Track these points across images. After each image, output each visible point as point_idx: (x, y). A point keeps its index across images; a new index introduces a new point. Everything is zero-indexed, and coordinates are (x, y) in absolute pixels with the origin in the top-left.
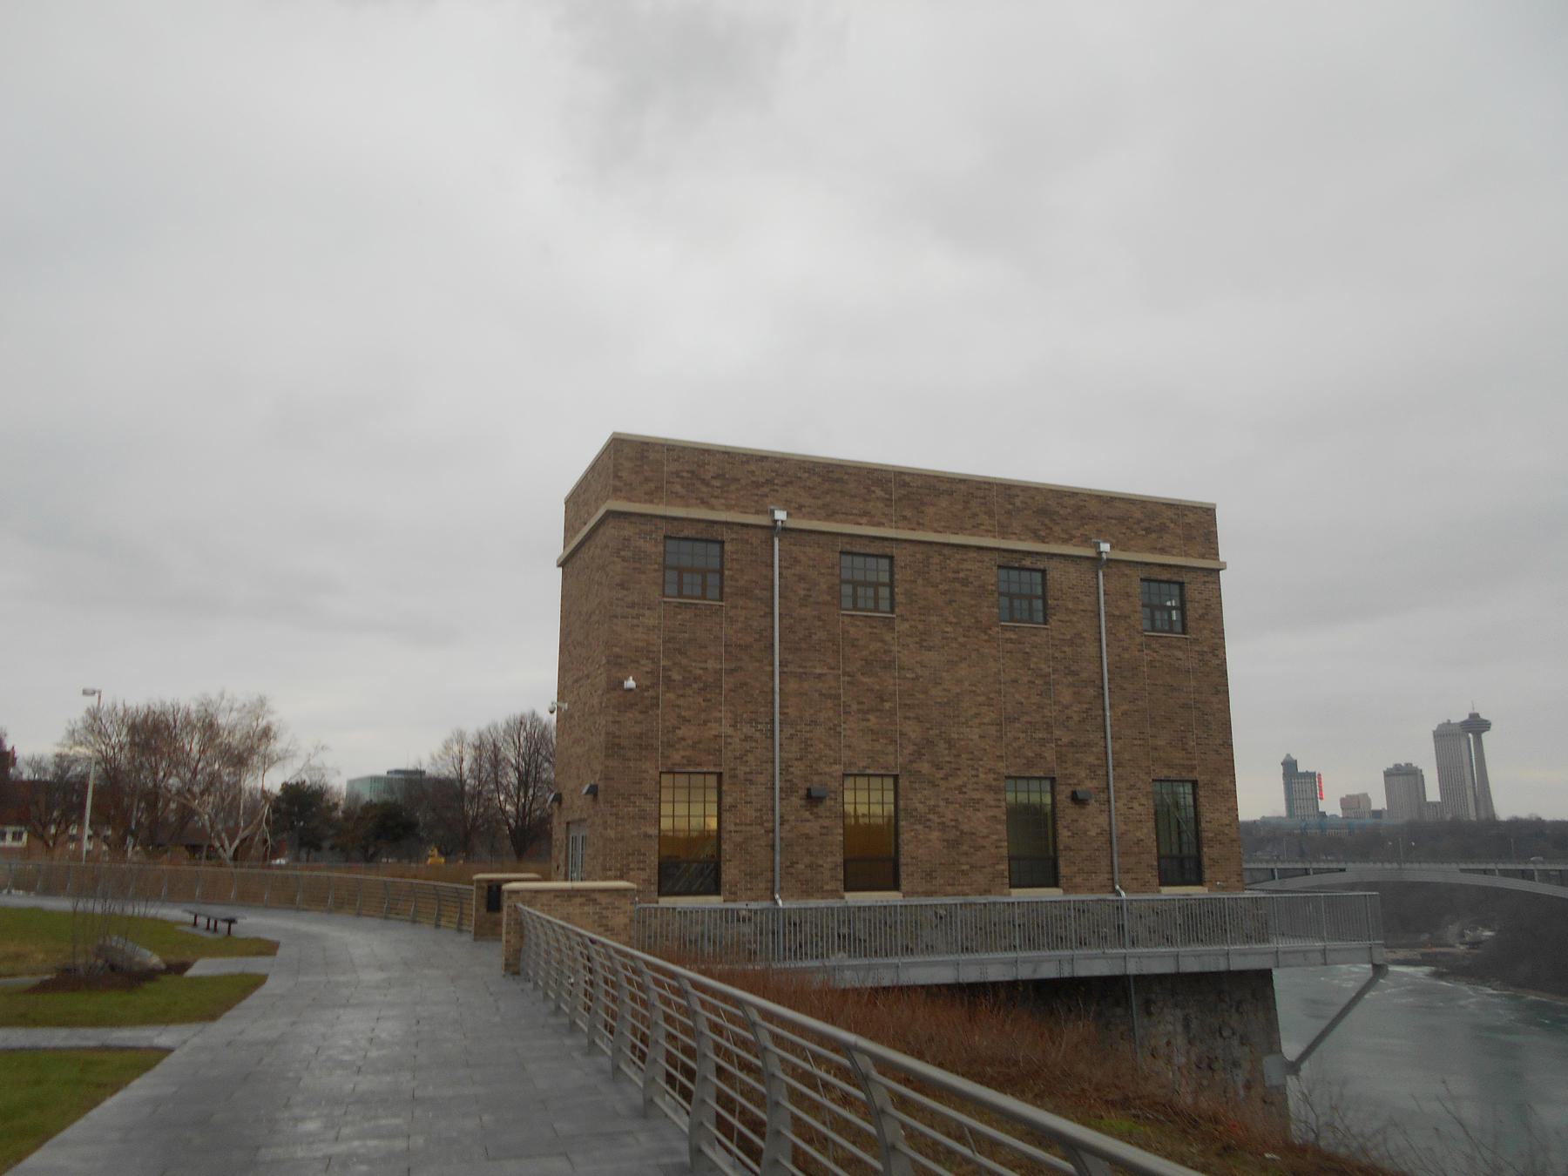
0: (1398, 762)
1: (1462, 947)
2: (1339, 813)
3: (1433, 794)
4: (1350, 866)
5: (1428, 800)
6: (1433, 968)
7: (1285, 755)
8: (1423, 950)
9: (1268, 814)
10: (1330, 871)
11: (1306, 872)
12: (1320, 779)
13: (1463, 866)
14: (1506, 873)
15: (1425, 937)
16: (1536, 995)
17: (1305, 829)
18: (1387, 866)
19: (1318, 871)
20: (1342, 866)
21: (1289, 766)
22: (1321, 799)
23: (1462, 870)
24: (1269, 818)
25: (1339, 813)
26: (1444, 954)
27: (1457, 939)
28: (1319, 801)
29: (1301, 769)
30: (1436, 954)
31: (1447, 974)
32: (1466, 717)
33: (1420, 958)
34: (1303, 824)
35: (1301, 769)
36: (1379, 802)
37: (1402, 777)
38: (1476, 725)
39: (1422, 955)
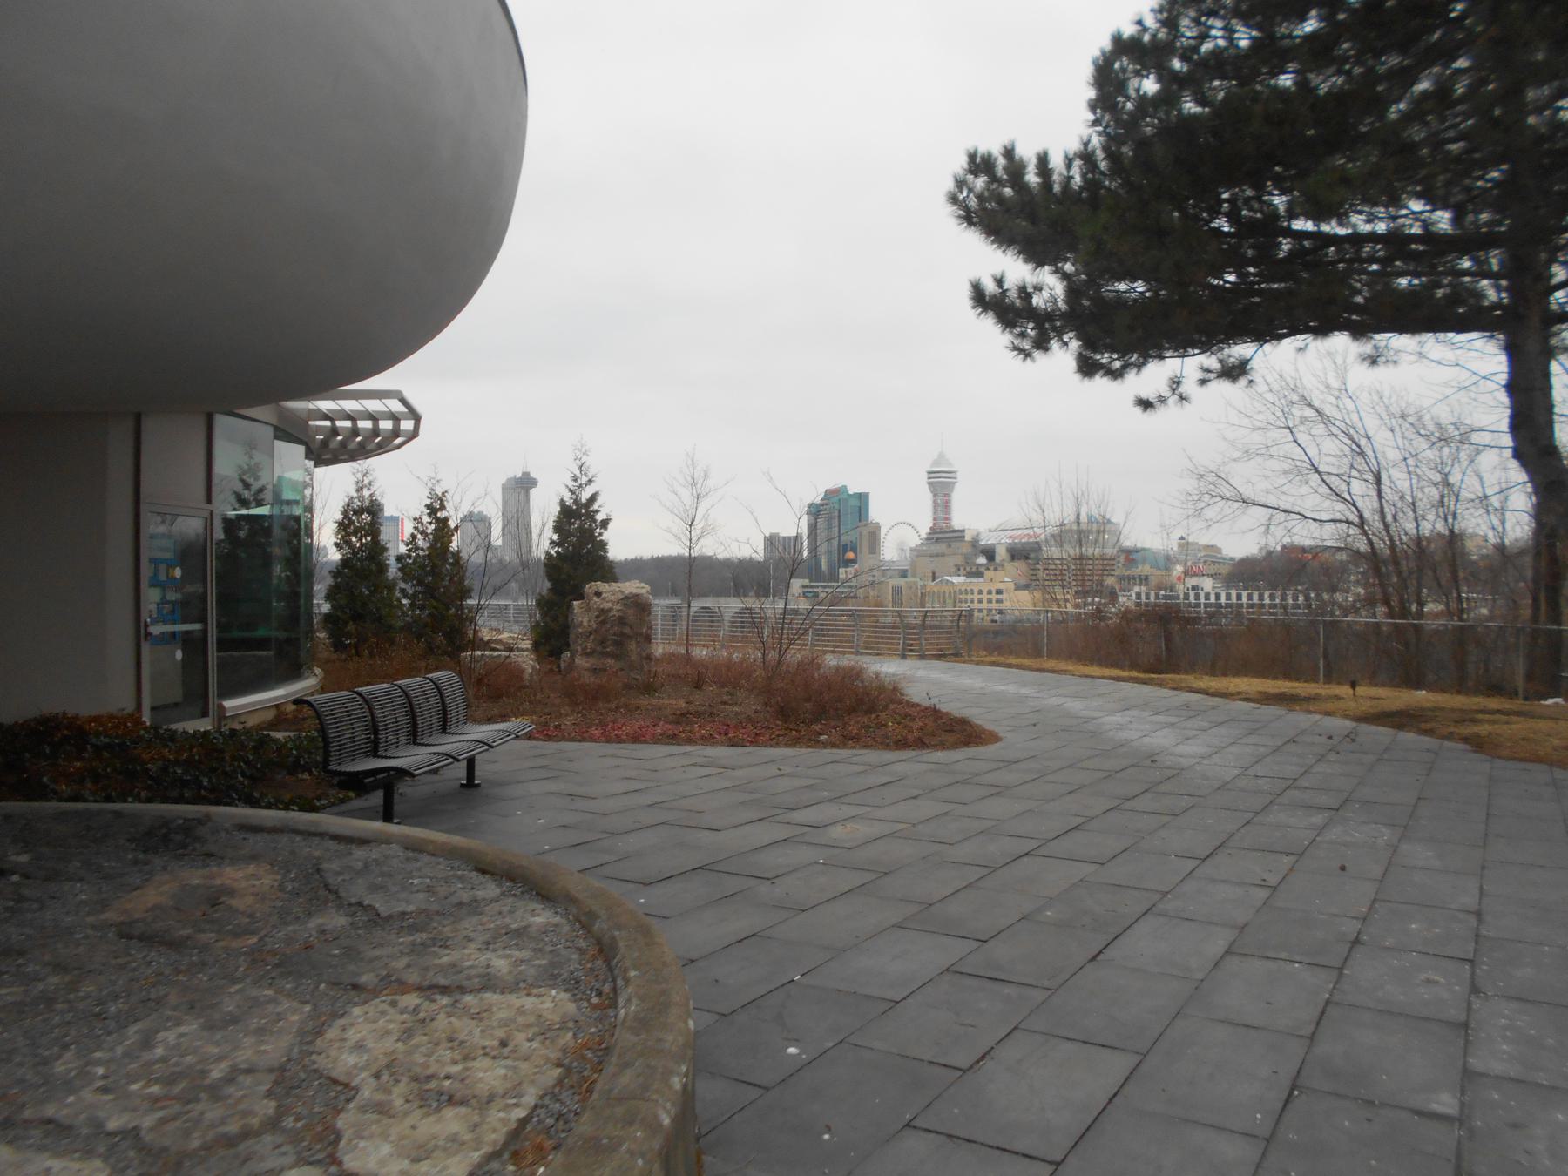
32: (519, 475)
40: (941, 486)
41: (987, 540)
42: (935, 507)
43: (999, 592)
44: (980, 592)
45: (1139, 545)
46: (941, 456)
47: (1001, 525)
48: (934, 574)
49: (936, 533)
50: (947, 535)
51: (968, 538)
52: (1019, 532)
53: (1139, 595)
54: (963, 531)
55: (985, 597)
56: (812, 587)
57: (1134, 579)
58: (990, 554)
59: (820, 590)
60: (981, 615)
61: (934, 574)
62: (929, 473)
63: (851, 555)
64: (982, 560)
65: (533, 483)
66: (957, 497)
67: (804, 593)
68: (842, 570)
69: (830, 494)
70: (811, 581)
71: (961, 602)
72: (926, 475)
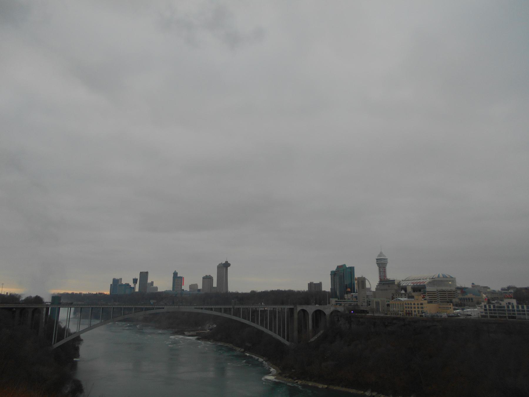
0: (207, 275)
1: (208, 330)
3: (215, 285)
4: (165, 307)
5: (213, 286)
6: (198, 337)
8: (197, 332)
9: (168, 289)
12: (183, 279)
13: (195, 307)
14: (206, 309)
15: (200, 328)
16: (220, 343)
17: (176, 294)
18: (176, 307)
20: (163, 307)
21: (175, 274)
22: (183, 285)
23: (195, 308)
24: (168, 291)
25: (188, 290)
26: (202, 333)
27: (208, 328)
28: (182, 286)
29: (178, 276)
30: (200, 333)
31: (201, 338)
32: (224, 262)
33: (196, 334)
35: (178, 276)
36: (200, 287)
37: (207, 279)
38: (227, 265)
39: (197, 333)
40: (382, 264)
41: (404, 284)
42: (380, 272)
43: (422, 304)
44: (414, 304)
45: (463, 286)
46: (381, 253)
47: (407, 278)
49: (383, 281)
50: (388, 282)
51: (396, 283)
52: (416, 281)
53: (485, 306)
54: (394, 280)
55: (416, 306)
56: (339, 301)
57: (469, 299)
58: (405, 289)
59: (342, 303)
60: (415, 313)
62: (377, 259)
63: (349, 290)
64: (403, 292)
66: (388, 268)
68: (346, 295)
69: (339, 267)
70: (338, 299)
71: (406, 308)
72: (376, 260)
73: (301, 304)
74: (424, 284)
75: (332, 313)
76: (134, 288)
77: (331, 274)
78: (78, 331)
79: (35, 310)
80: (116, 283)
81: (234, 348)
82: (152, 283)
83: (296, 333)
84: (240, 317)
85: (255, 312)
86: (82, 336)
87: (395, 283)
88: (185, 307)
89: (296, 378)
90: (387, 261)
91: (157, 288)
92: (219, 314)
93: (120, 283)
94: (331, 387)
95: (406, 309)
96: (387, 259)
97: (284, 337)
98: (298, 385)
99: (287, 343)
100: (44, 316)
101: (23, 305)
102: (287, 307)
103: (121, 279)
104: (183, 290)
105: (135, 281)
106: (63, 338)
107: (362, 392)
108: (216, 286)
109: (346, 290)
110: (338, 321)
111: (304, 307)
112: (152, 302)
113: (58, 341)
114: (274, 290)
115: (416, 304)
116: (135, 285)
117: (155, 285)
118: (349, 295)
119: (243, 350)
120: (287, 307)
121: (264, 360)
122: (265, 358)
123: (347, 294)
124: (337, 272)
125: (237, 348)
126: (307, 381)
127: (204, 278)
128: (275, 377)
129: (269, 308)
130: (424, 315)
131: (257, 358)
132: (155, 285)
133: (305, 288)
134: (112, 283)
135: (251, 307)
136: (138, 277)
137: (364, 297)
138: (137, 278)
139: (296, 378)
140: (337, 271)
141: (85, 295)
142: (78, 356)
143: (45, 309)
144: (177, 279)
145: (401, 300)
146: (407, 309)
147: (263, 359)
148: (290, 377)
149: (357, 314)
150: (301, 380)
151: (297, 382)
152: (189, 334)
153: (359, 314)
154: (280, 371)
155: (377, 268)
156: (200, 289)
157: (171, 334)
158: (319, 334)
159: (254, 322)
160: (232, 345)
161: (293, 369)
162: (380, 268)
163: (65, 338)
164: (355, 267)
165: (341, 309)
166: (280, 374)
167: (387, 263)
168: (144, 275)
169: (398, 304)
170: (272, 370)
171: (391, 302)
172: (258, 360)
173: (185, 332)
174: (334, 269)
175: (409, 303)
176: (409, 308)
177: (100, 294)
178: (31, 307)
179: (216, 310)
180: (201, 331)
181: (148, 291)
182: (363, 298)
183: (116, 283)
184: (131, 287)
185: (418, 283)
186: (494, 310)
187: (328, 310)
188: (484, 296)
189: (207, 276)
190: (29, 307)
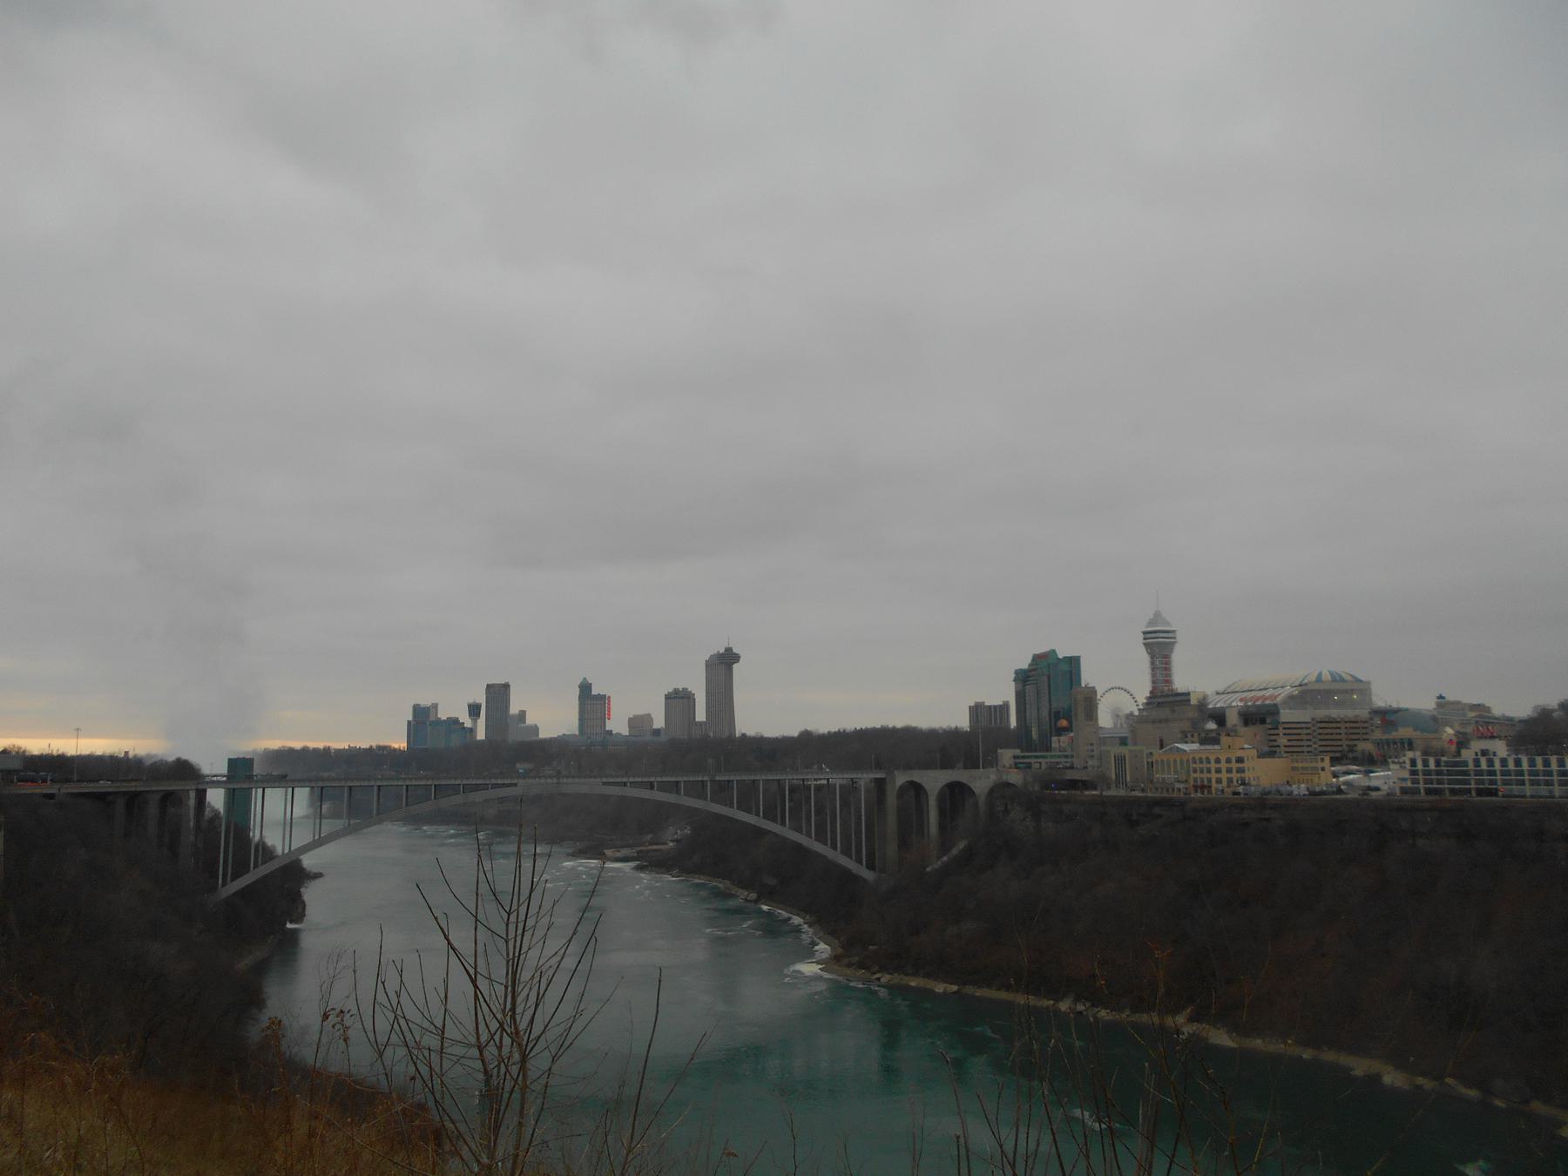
1: (671, 844)
2: (625, 731)
3: (701, 716)
4: (521, 782)
5: (697, 720)
6: (638, 862)
7: (582, 679)
10: (504, 785)
11: (485, 787)
12: (609, 701)
13: (604, 780)
16: (700, 879)
19: (495, 786)
20: (515, 781)
21: (585, 688)
25: (625, 731)
27: (672, 837)
30: (648, 851)
32: (722, 651)
33: (635, 855)
34: (589, 741)
36: (659, 722)
37: (679, 700)
39: (638, 852)
40: (1159, 646)
41: (1215, 703)
42: (1154, 668)
43: (1240, 760)
44: (1218, 761)
45: (1395, 705)
46: (1157, 615)
47: (1229, 687)
48: (1161, 741)
49: (1157, 697)
50: (1170, 699)
51: (1193, 701)
52: (1253, 694)
53: (1413, 762)
54: (1188, 694)
55: (1223, 766)
56: (1023, 757)
57: (1395, 743)
58: (1219, 716)
59: (1033, 760)
60: (1220, 787)
61: (1161, 741)
62: (1145, 633)
63: (1064, 723)
64: (1212, 726)
65: (736, 658)
66: (1178, 658)
67: (1016, 764)
68: (1054, 739)
69: (1037, 659)
70: (1022, 752)
71: (1195, 771)
72: (1142, 636)
73: (909, 767)
74: (1275, 702)
75: (991, 791)
76: (472, 731)
77: (1014, 681)
78: (286, 851)
79: (168, 798)
80: (422, 719)
81: (733, 892)
82: (522, 714)
83: (892, 848)
84: (731, 806)
85: (799, 791)
86: (309, 861)
87: (1189, 700)
88: (577, 780)
89: (876, 968)
90: (1175, 638)
91: (535, 729)
92: (671, 798)
93: (432, 718)
94: (969, 990)
95: (1195, 775)
96: (1174, 632)
97: (859, 861)
98: (879, 986)
99: (868, 875)
100: (192, 814)
101: (134, 784)
102: (865, 778)
103: (435, 706)
104: (610, 732)
105: (474, 710)
106: (248, 871)
107: (1052, 1002)
108: (705, 720)
109: (1056, 723)
110: (1006, 811)
111: (917, 776)
112: (521, 767)
113: (235, 877)
114: (869, 727)
115: (1212, 761)
116: (475, 722)
117: (530, 721)
118: (1062, 738)
119: (753, 896)
120: (865, 778)
121: (807, 923)
122: (808, 917)
123: (1059, 735)
124: (1033, 673)
125: (740, 891)
126: (906, 975)
127: (668, 697)
128: (820, 966)
129: (838, 779)
130: (1244, 789)
131: (785, 914)
132: (530, 721)
133: (963, 722)
134: (411, 719)
135: (790, 778)
136: (481, 699)
137: (1092, 745)
138: (478, 701)
139: (876, 968)
140: (1031, 671)
141: (338, 751)
142: (300, 917)
143: (192, 795)
144: (591, 703)
145: (1185, 751)
146: (1197, 775)
147: (804, 918)
148: (861, 965)
149: (1056, 792)
150: (889, 974)
151: (879, 979)
152: (618, 855)
153: (1063, 792)
154: (840, 951)
155: (1143, 658)
156: (659, 727)
157: (568, 855)
158: (955, 851)
159: (774, 820)
160: (728, 882)
161: (873, 945)
162: (1152, 657)
163: (252, 869)
164: (1081, 659)
165: (1015, 777)
166: (836, 958)
167: (1173, 643)
168: (498, 694)
169: (1175, 761)
170: (822, 946)
171: (1158, 754)
172: (790, 919)
173: (605, 851)
174: (1025, 664)
175: (1204, 757)
176: (1202, 772)
177: (380, 748)
178: (154, 789)
179: (665, 787)
180: (650, 847)
181: (514, 736)
182: (1090, 748)
183: (422, 719)
184: (464, 728)
185: (1258, 699)
186: (1439, 773)
187: (981, 782)
188: (1450, 731)
189: (676, 691)
190: (148, 789)
